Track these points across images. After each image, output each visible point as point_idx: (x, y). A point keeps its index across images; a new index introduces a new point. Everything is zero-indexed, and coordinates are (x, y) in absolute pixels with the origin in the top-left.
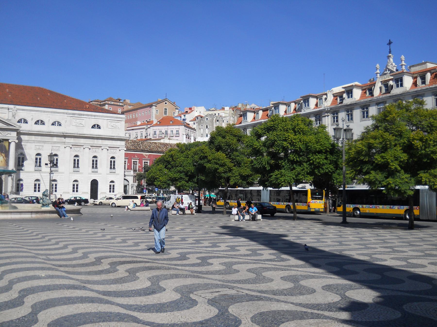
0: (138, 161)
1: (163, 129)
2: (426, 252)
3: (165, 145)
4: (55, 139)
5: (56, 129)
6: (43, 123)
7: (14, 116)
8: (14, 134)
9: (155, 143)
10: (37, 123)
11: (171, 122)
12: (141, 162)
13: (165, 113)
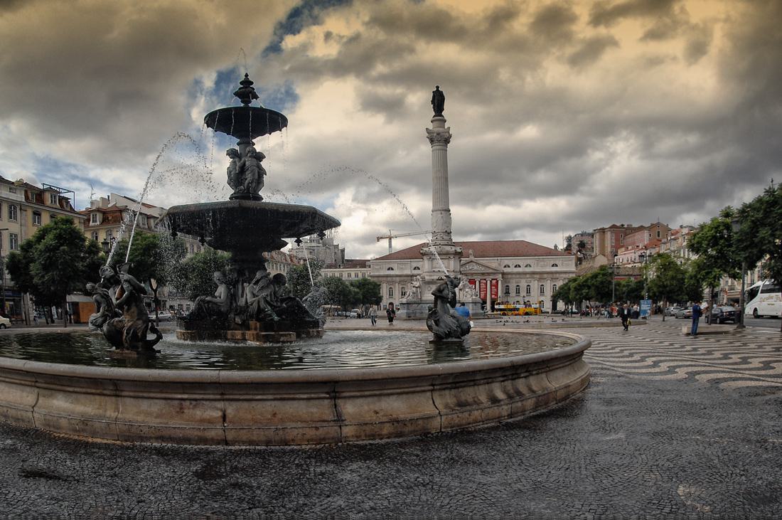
4: (528, 276)
5: (528, 270)
6: (519, 266)
7: (500, 265)
8: (500, 275)
10: (516, 266)
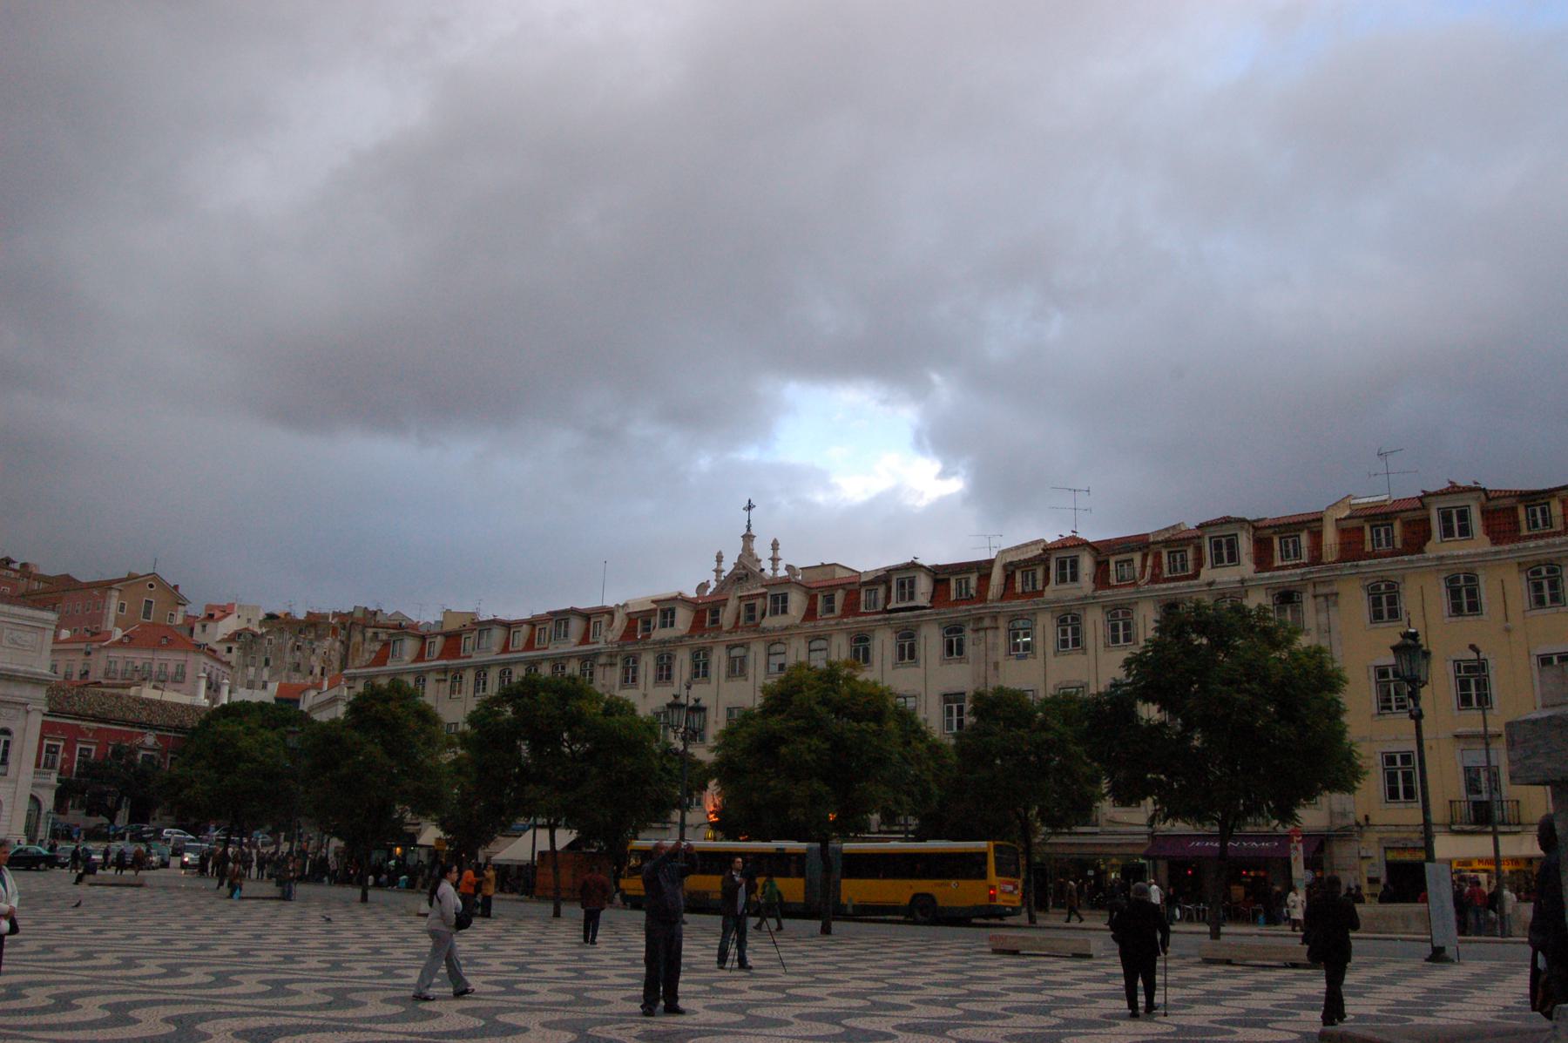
0: (62, 744)
1: (140, 657)
2: (874, 998)
3: (148, 703)
9: (119, 697)
11: (164, 642)
12: (69, 749)
13: (147, 614)
